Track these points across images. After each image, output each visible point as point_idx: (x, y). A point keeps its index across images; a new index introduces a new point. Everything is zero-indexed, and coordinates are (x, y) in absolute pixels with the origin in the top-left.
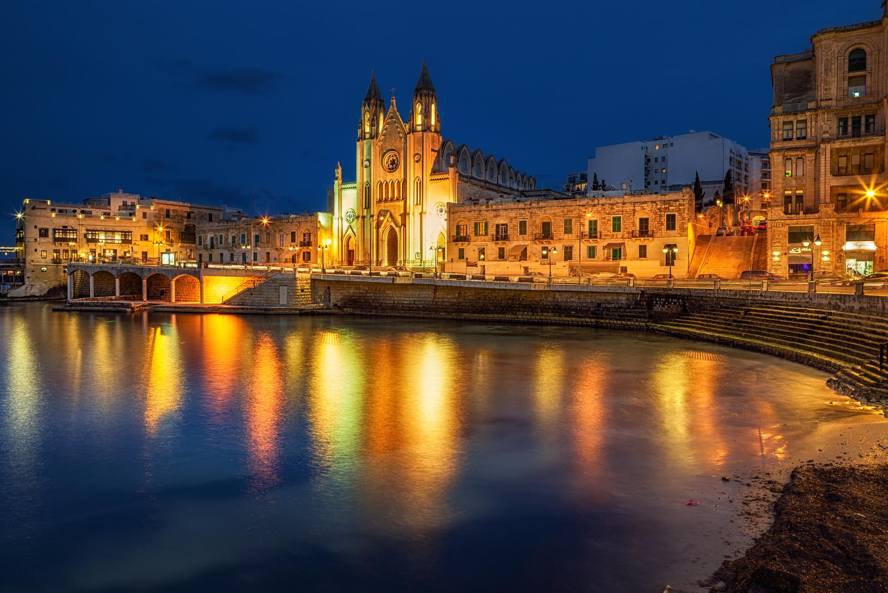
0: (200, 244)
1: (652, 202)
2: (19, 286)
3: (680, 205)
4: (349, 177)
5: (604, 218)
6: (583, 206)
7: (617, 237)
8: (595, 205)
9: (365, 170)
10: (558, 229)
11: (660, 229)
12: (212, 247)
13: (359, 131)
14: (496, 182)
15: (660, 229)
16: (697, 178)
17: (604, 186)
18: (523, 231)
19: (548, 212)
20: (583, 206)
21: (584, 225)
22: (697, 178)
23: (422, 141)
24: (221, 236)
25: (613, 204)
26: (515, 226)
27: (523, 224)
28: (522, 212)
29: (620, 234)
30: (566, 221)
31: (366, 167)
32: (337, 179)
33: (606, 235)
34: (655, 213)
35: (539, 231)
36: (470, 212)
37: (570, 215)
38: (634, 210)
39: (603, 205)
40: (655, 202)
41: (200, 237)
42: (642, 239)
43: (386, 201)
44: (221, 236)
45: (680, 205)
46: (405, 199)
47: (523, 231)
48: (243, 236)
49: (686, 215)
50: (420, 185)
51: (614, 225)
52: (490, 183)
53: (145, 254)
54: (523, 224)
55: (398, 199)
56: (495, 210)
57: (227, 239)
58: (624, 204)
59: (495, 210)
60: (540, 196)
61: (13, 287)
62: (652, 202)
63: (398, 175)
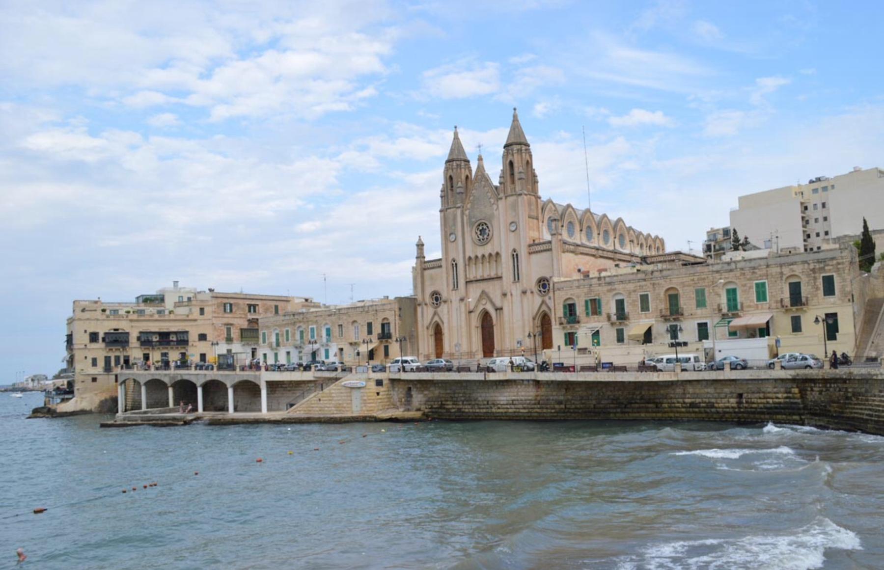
0: (264, 342)
2: (68, 399)
3: (839, 264)
5: (745, 285)
6: (717, 272)
7: (762, 308)
8: (731, 271)
10: (687, 303)
11: (816, 296)
12: (278, 344)
14: (611, 248)
16: (865, 227)
17: (746, 243)
18: (645, 307)
19: (675, 281)
20: (717, 272)
21: (719, 295)
22: (865, 227)
23: (515, 207)
24: (287, 331)
25: (754, 268)
26: (634, 301)
27: (644, 299)
28: (643, 283)
30: (697, 292)
33: (750, 306)
34: (808, 275)
35: (664, 306)
36: (578, 287)
37: (701, 285)
39: (742, 269)
41: (264, 334)
42: (794, 308)
44: (287, 331)
45: (839, 264)
47: (645, 307)
48: (312, 329)
49: (847, 277)
52: (604, 250)
53: (203, 357)
54: (644, 299)
56: (609, 284)
57: (294, 335)
58: (768, 266)
59: (609, 284)
60: (665, 261)
61: (63, 400)
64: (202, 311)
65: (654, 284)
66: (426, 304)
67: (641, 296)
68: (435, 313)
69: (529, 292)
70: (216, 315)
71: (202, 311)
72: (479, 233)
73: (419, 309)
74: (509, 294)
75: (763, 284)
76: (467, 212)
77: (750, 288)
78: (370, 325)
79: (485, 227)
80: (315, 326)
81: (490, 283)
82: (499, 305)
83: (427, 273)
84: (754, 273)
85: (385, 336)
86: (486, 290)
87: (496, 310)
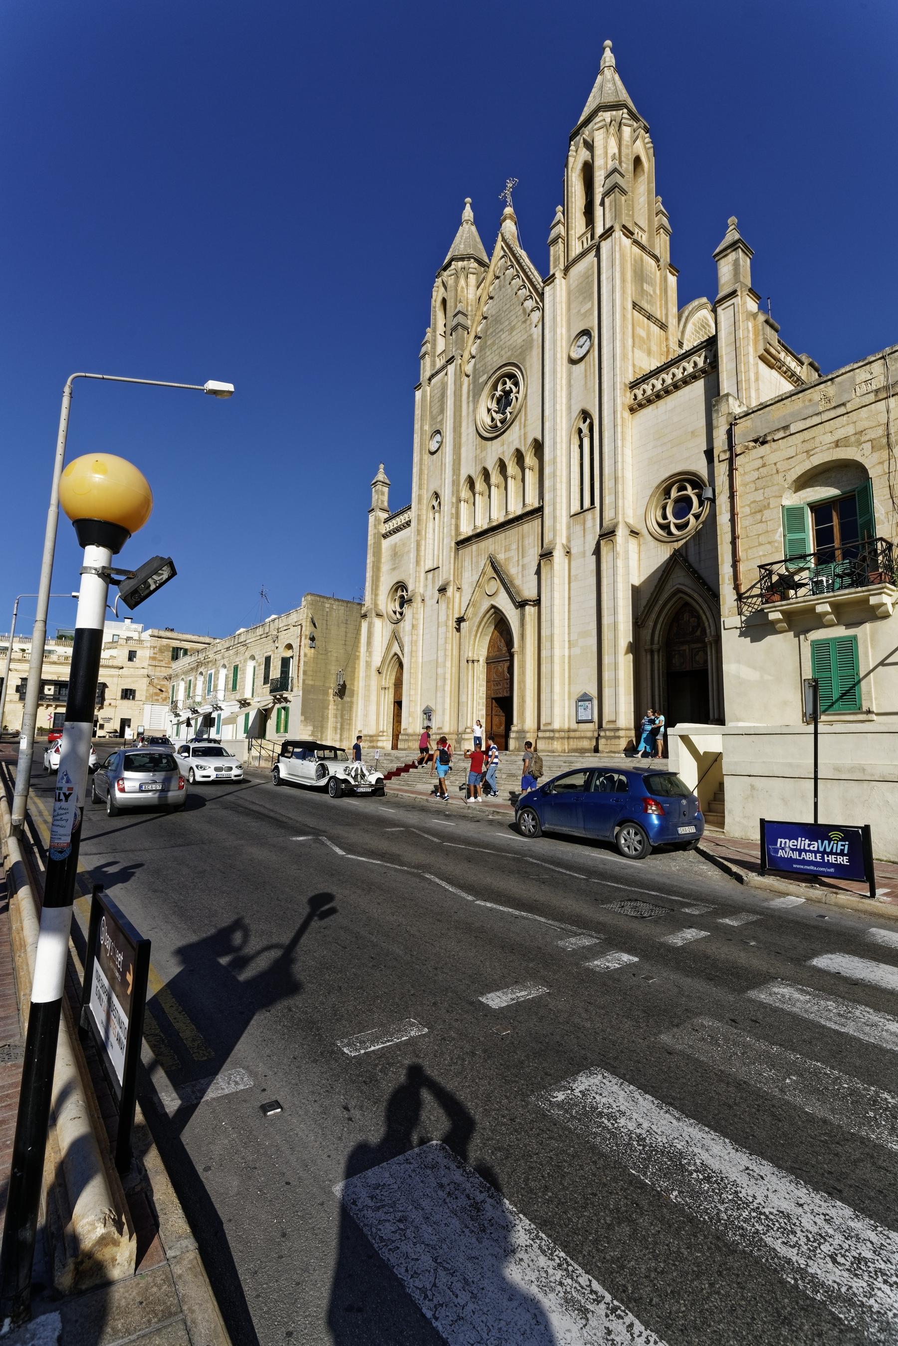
48: (211, 675)
64: (132, 656)
66: (379, 615)
68: (396, 637)
69: (621, 533)
70: (154, 663)
71: (132, 656)
72: (494, 406)
73: (364, 625)
74: (558, 555)
76: (469, 368)
78: (268, 660)
80: (213, 671)
81: (512, 534)
82: (529, 592)
83: (386, 544)
85: (280, 686)
86: (501, 557)
87: (521, 605)
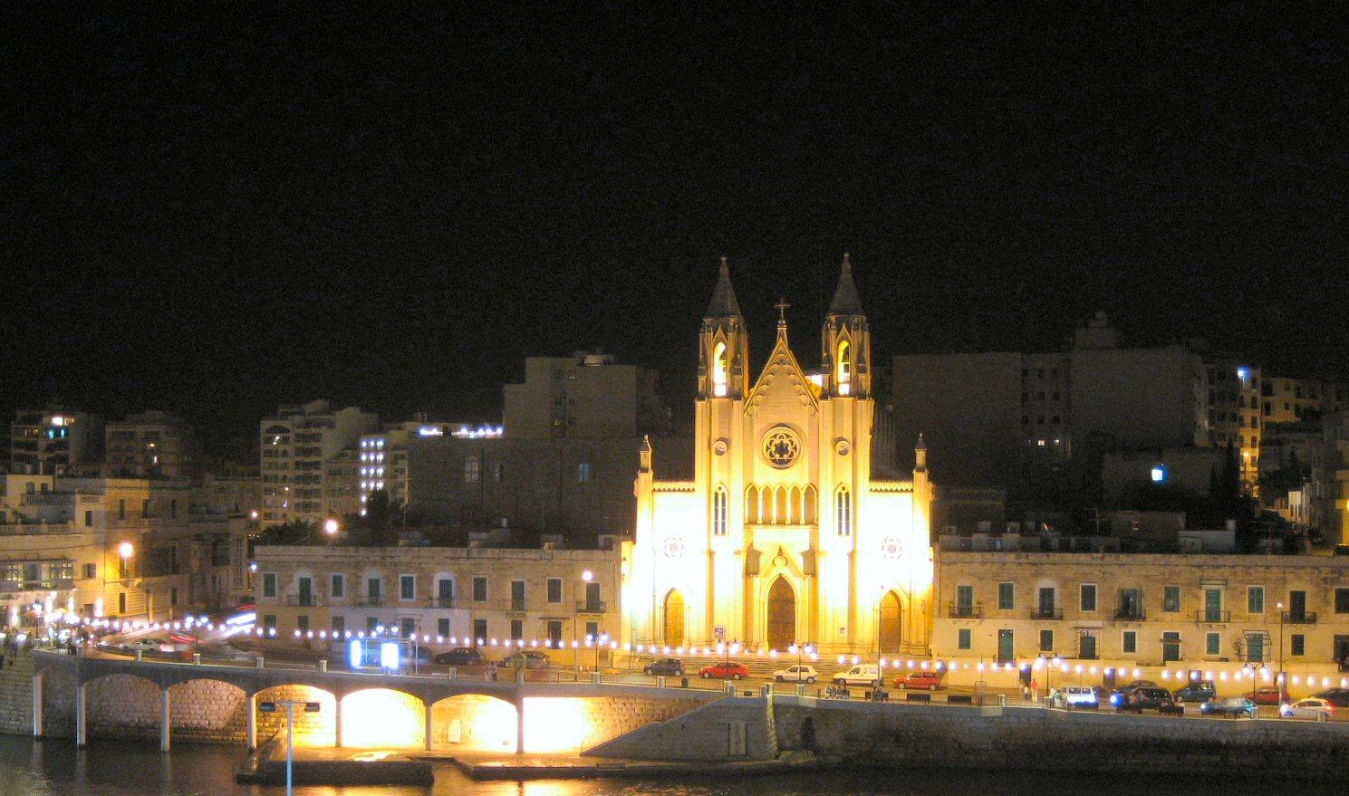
1: (1313, 568)
4: (677, 467)
6: (1199, 566)
9: (715, 458)
10: (1150, 604)
11: (1326, 611)
13: (702, 379)
15: (1326, 611)
29: (1260, 616)
31: (719, 453)
32: (645, 470)
35: (1114, 605)
36: (983, 563)
38: (1284, 578)
40: (1317, 568)
43: (781, 523)
46: (812, 522)
50: (845, 500)
51: (1251, 601)
55: (796, 523)
56: (1035, 564)
59: (1035, 564)
62: (1313, 568)
63: (796, 476)
65: (1104, 573)
67: (1084, 589)
75: (1260, 591)
77: (1242, 593)
79: (786, 441)
84: (1248, 574)
